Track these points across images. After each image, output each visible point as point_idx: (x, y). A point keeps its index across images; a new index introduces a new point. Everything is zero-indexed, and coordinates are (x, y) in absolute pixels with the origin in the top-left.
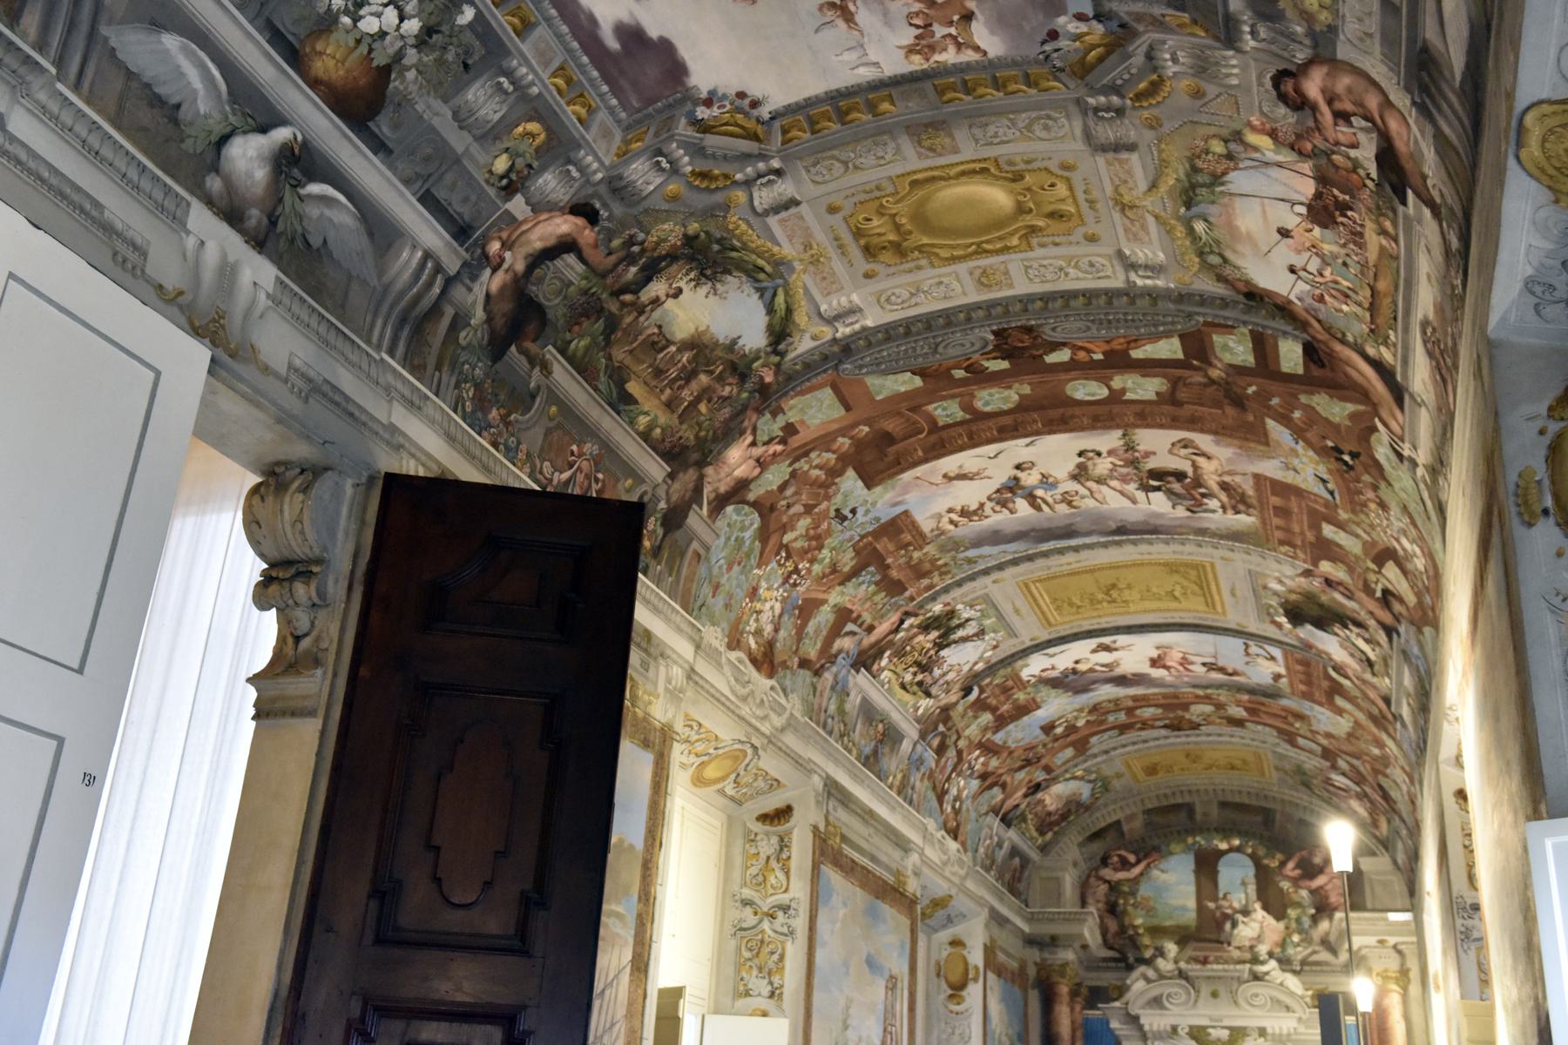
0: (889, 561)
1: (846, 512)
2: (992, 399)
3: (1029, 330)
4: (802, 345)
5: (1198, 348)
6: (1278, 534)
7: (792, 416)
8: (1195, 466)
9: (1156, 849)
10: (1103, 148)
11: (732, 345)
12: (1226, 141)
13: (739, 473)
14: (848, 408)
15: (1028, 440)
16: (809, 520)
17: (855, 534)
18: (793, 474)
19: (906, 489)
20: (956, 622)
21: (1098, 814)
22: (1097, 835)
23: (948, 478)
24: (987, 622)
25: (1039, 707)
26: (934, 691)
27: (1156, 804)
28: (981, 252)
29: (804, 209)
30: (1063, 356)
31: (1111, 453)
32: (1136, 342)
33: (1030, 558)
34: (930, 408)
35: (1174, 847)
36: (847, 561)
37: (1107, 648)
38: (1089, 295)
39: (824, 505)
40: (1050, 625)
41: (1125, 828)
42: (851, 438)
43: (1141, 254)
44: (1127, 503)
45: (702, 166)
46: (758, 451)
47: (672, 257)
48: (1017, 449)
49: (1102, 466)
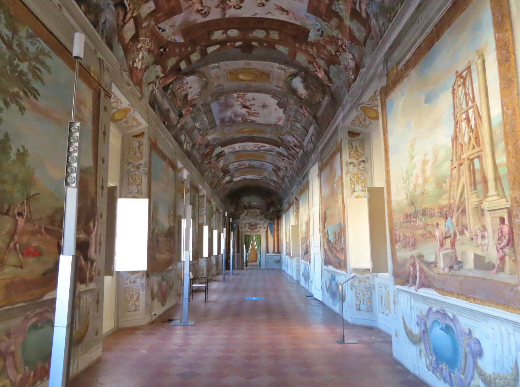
1: (320, 33)
4: (292, 70)
5: (204, 53)
10: (221, 85)
11: (302, 82)
13: (323, 74)
17: (324, 24)
18: (318, 57)
23: (287, 12)
28: (248, 69)
30: (238, 44)
31: (230, 7)
32: (218, 49)
34: (278, 38)
36: (334, 21)
38: (228, 60)
39: (322, 42)
42: (301, 46)
43: (216, 70)
46: (317, 69)
47: (297, 96)
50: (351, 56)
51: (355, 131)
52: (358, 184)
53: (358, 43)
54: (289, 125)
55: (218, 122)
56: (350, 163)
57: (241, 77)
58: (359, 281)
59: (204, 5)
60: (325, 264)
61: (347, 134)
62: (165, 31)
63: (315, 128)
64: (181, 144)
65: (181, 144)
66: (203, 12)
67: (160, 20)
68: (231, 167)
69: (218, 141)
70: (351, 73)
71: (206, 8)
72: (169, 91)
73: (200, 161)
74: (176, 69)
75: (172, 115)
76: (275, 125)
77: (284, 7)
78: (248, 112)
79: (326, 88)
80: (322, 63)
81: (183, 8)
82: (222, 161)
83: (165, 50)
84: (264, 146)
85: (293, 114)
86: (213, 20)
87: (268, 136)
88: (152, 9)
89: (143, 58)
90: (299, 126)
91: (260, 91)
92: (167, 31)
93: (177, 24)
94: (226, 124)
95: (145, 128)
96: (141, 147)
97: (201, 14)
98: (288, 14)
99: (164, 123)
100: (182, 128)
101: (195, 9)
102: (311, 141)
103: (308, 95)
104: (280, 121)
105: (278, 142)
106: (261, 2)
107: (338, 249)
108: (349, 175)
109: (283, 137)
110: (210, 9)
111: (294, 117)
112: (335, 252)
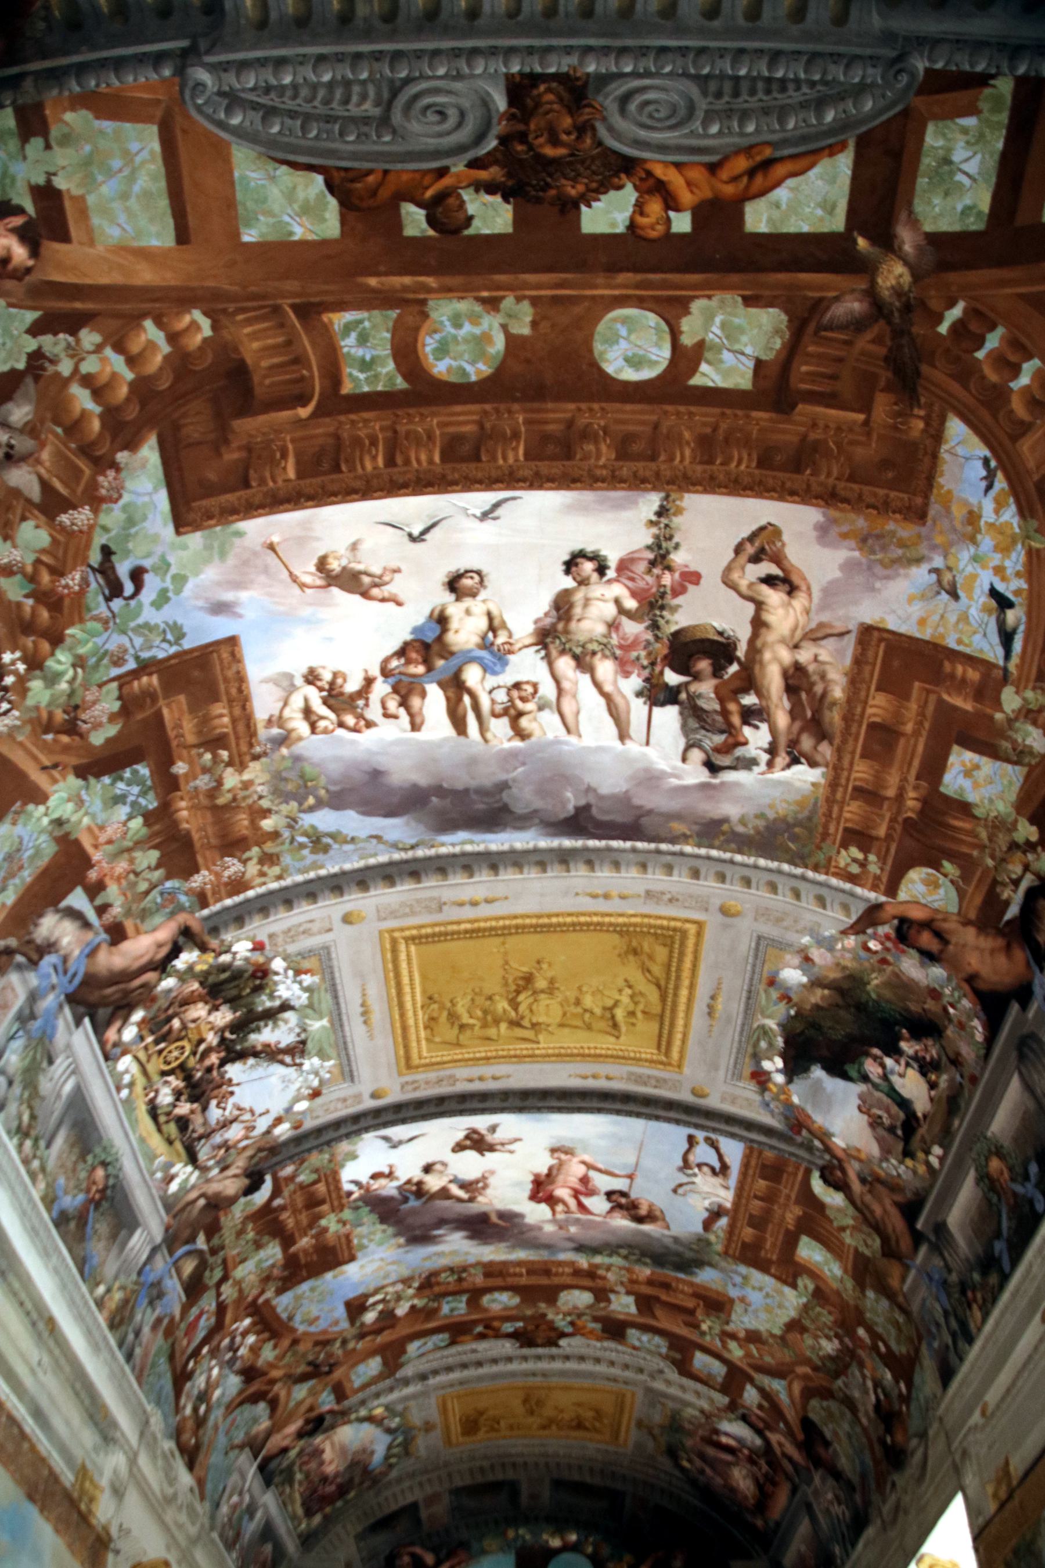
0: (180, 768)
1: (123, 569)
6: (853, 811)
8: (758, 624)
9: (464, 1545)
14: (182, 236)
15: (484, 499)
20: (264, 1002)
21: (388, 1493)
22: (385, 1523)
24: (318, 1025)
25: (352, 1258)
26: (204, 1152)
27: (468, 1481)
31: (623, 566)
33: (413, 870)
35: (488, 1543)
37: (477, 1143)
40: (409, 1066)
41: (424, 1514)
59: (750, 608)
62: (993, 593)
66: (767, 568)
67: (973, 675)
71: (743, 584)
81: (849, 644)
92: (986, 578)
93: (921, 575)
97: (778, 559)
98: (322, 565)
101: (799, 602)
106: (468, 602)
110: (728, 569)
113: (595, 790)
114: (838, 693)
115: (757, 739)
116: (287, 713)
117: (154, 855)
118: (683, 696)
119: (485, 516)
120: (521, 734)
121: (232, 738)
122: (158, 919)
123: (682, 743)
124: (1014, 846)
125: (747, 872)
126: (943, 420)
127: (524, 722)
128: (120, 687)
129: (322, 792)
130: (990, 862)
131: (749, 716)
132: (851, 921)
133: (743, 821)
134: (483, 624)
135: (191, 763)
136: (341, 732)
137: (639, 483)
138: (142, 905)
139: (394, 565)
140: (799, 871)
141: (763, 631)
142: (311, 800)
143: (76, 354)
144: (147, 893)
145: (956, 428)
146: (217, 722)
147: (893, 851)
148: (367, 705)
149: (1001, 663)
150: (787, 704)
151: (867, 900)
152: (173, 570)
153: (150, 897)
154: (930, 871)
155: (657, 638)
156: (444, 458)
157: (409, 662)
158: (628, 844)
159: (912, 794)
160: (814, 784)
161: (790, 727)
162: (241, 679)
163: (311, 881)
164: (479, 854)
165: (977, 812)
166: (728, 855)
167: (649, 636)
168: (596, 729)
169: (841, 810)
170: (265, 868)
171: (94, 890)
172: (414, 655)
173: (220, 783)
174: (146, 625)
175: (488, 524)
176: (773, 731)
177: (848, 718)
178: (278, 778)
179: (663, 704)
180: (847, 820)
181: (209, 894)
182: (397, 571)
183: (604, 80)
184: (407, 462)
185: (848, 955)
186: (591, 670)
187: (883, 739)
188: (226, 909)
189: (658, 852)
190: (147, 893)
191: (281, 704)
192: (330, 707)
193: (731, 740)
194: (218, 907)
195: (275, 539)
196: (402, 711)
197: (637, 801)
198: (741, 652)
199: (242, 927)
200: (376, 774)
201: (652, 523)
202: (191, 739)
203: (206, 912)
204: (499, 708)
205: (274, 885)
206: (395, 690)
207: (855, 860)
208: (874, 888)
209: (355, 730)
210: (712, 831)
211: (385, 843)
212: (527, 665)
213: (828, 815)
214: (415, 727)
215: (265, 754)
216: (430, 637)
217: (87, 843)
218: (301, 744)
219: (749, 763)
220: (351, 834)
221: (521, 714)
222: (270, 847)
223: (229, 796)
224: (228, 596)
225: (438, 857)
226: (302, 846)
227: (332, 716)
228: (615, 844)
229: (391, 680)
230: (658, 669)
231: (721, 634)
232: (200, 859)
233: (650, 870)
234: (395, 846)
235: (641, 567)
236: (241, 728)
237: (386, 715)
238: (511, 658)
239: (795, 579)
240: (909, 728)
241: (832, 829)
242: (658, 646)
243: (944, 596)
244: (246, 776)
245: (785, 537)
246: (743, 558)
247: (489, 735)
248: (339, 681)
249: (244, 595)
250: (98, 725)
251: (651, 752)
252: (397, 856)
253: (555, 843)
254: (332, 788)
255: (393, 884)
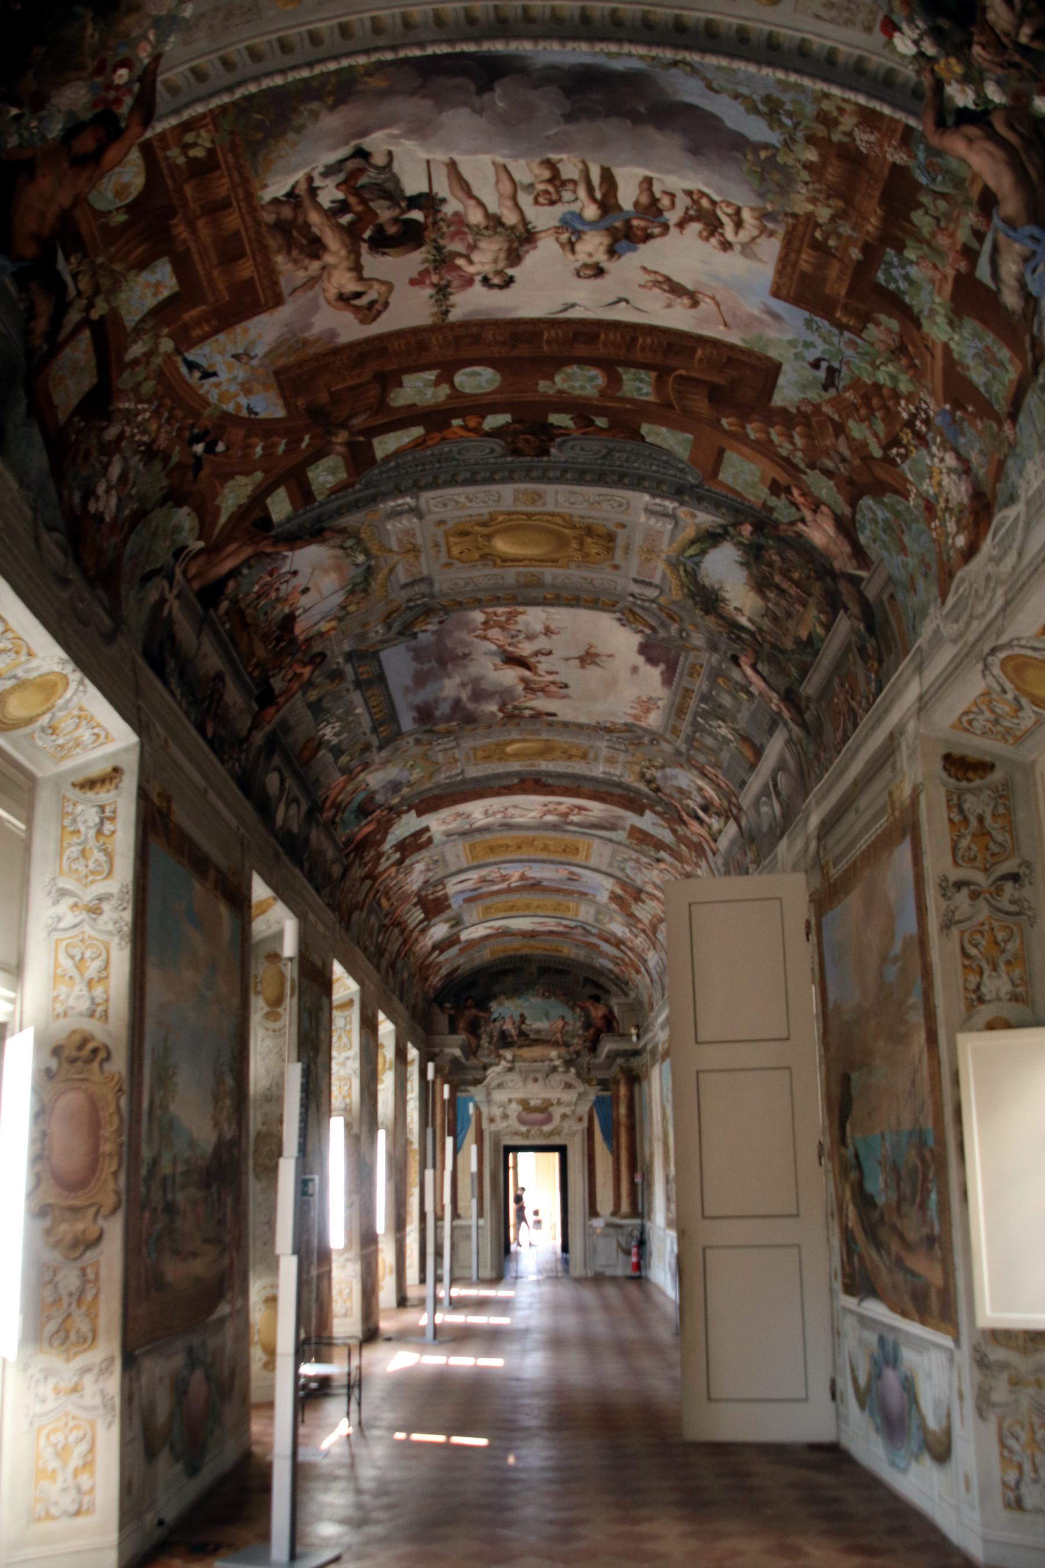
0: (855, 254)
1: (822, 374)
2: (582, 381)
3: (516, 452)
4: (706, 519)
5: (359, 458)
6: (222, 187)
7: (764, 492)
8: (357, 268)
10: (422, 580)
11: (745, 564)
12: (348, 613)
13: (831, 530)
14: (721, 451)
15: (571, 314)
16: (851, 424)
17: (840, 340)
18: (812, 466)
19: (752, 321)
28: (529, 515)
29: (633, 574)
30: (494, 421)
31: (469, 282)
32: (418, 444)
34: (652, 398)
36: (884, 329)
38: (453, 482)
39: (827, 409)
42: (744, 427)
44: (467, 166)
45: (668, 621)
46: (807, 514)
47: (721, 617)
48: (587, 301)
49: (486, 257)
50: (950, 460)
51: (973, 755)
52: (995, 968)
53: (985, 409)
54: (685, 727)
55: (407, 721)
56: (959, 885)
57: (502, 545)
58: (1015, 1383)
59: (366, 274)
60: (850, 1289)
61: (938, 765)
63: (789, 741)
64: (264, 808)
65: (264, 808)
66: (363, 301)
68: (452, 888)
69: (405, 790)
70: (951, 526)
71: (376, 286)
72: (225, 605)
73: (336, 870)
74: (254, 521)
75: (233, 696)
76: (629, 728)
77: (677, 278)
78: (523, 680)
79: (843, 586)
80: (824, 488)
81: (285, 286)
82: (420, 867)
83: (210, 448)
84: (581, 808)
85: (700, 684)
86: (398, 334)
87: (598, 771)
88: (165, 293)
89: (123, 478)
90: (724, 731)
91: (574, 601)
92: (223, 376)
93: (260, 350)
94: (441, 727)
95: (126, 750)
96: (108, 827)
97: (357, 309)
98: (695, 304)
99: (201, 729)
100: (273, 743)
101: (332, 292)
102: (771, 789)
103: (767, 613)
104: (647, 711)
105: (637, 792)
107: (912, 1236)
108: (955, 931)
109: (658, 774)
111: (705, 698)
112: (895, 1246)
113: (474, 111)
114: (280, 259)
115: (329, 194)
116: (755, 232)
117: (917, 216)
118: (403, 204)
119: (573, 306)
120: (550, 165)
121: (806, 242)
122: (954, 164)
123: (396, 168)
124: (97, 290)
125: (290, 60)
126: (289, 411)
127: (547, 174)
128: (862, 331)
129: (750, 157)
130: (100, 260)
131: (343, 207)
132: (160, 79)
133: (315, 115)
134: (579, 247)
135: (846, 249)
136: (717, 198)
137: (463, 324)
138: (954, 192)
139: (642, 290)
140: (239, 93)
141: (352, 265)
142: (763, 155)
143: (792, 452)
144: (943, 196)
145: (280, 413)
146: (811, 260)
147: (169, 182)
148: (687, 209)
149: (186, 355)
150: (315, 230)
151: (161, 119)
152: (794, 351)
153: (945, 190)
154: (131, 198)
155: (435, 241)
156: (598, 336)
157: (645, 229)
158: (429, 51)
159: (185, 235)
160: (266, 186)
161: (306, 216)
162: (780, 272)
163: (798, 72)
164: (602, 39)
165: (134, 272)
166: (318, 70)
167: (442, 242)
168: (480, 168)
169: (232, 181)
170: (835, 114)
171: (970, 254)
172: (639, 233)
173: (833, 218)
174: (825, 341)
175: (570, 300)
176: (318, 206)
177: (264, 249)
178: (785, 189)
179: (420, 195)
180: (222, 176)
181: (898, 135)
182: (640, 286)
183: (504, 456)
184: (623, 337)
185: (136, 33)
186: (487, 215)
187: (230, 251)
188: (893, 105)
189: (394, 48)
190: (943, 196)
191: (758, 241)
192: (719, 220)
193: (352, 183)
194: (899, 116)
195: (722, 328)
196: (658, 195)
197: (428, 103)
198: (364, 248)
199: (891, 72)
200: (695, 151)
201: (452, 306)
202: (836, 265)
203: (912, 122)
204: (570, 186)
205: (836, 91)
206: (660, 212)
207: (194, 145)
208: (162, 136)
209: (703, 194)
210: (342, 90)
211: (704, 79)
212: (543, 218)
213: (240, 168)
214: (648, 181)
215: (786, 214)
216: (624, 243)
217: (948, 288)
218: (752, 204)
219: (329, 171)
220: (736, 104)
221: (550, 181)
222: (821, 131)
223: (831, 202)
224: (766, 317)
225: (648, 43)
226: (790, 115)
227: (719, 213)
228: (444, 49)
229: (662, 220)
230: (430, 220)
231: (384, 254)
232: (886, 172)
233: (398, 20)
234: (694, 70)
235: (455, 283)
236: (796, 244)
237: (672, 196)
238: (556, 223)
239: (340, 304)
240: (216, 273)
241: (230, 158)
242: (434, 236)
243: (241, 351)
244: (810, 207)
245: (356, 322)
246: (382, 300)
247: (580, 166)
248: (705, 234)
249: (756, 312)
250: (889, 331)
251: (423, 155)
252: (695, 58)
253: (514, 47)
254: (740, 156)
255: (709, 23)
